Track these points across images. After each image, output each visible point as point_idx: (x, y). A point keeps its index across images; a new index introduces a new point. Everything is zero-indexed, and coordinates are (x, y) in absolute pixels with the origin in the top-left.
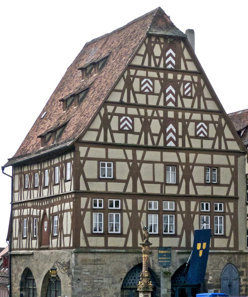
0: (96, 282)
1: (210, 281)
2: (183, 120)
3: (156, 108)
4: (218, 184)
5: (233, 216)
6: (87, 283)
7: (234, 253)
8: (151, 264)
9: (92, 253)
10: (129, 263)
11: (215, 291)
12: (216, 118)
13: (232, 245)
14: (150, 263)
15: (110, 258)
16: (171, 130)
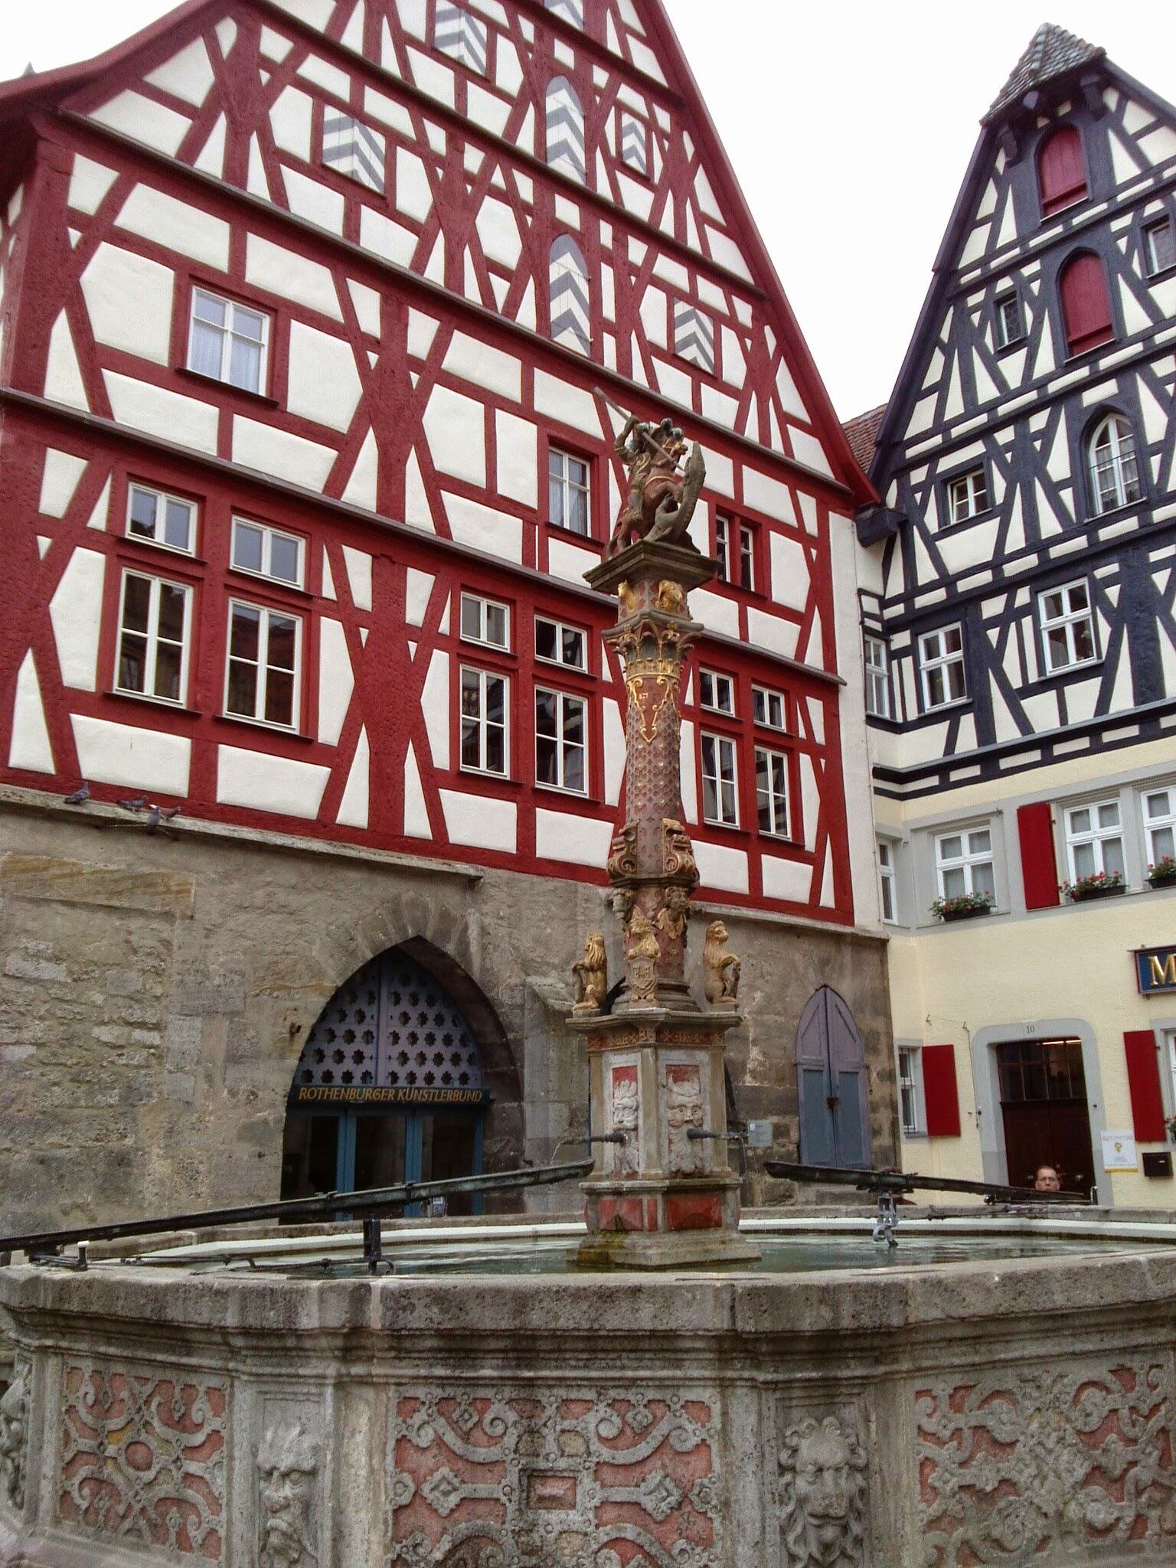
0: (104, 1038)
1: (753, 1073)
2: (616, 258)
3: (500, 150)
4: (762, 600)
5: (823, 761)
6: (39, 1045)
7: (838, 938)
8: (474, 948)
9: (97, 827)
10: (347, 931)
11: (779, 1132)
12: (744, 312)
13: (827, 899)
14: (467, 945)
15: (226, 877)
16: (567, 281)
